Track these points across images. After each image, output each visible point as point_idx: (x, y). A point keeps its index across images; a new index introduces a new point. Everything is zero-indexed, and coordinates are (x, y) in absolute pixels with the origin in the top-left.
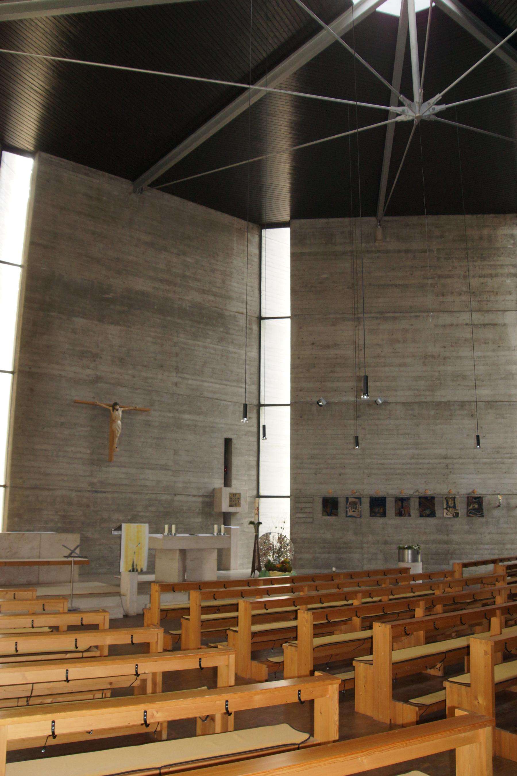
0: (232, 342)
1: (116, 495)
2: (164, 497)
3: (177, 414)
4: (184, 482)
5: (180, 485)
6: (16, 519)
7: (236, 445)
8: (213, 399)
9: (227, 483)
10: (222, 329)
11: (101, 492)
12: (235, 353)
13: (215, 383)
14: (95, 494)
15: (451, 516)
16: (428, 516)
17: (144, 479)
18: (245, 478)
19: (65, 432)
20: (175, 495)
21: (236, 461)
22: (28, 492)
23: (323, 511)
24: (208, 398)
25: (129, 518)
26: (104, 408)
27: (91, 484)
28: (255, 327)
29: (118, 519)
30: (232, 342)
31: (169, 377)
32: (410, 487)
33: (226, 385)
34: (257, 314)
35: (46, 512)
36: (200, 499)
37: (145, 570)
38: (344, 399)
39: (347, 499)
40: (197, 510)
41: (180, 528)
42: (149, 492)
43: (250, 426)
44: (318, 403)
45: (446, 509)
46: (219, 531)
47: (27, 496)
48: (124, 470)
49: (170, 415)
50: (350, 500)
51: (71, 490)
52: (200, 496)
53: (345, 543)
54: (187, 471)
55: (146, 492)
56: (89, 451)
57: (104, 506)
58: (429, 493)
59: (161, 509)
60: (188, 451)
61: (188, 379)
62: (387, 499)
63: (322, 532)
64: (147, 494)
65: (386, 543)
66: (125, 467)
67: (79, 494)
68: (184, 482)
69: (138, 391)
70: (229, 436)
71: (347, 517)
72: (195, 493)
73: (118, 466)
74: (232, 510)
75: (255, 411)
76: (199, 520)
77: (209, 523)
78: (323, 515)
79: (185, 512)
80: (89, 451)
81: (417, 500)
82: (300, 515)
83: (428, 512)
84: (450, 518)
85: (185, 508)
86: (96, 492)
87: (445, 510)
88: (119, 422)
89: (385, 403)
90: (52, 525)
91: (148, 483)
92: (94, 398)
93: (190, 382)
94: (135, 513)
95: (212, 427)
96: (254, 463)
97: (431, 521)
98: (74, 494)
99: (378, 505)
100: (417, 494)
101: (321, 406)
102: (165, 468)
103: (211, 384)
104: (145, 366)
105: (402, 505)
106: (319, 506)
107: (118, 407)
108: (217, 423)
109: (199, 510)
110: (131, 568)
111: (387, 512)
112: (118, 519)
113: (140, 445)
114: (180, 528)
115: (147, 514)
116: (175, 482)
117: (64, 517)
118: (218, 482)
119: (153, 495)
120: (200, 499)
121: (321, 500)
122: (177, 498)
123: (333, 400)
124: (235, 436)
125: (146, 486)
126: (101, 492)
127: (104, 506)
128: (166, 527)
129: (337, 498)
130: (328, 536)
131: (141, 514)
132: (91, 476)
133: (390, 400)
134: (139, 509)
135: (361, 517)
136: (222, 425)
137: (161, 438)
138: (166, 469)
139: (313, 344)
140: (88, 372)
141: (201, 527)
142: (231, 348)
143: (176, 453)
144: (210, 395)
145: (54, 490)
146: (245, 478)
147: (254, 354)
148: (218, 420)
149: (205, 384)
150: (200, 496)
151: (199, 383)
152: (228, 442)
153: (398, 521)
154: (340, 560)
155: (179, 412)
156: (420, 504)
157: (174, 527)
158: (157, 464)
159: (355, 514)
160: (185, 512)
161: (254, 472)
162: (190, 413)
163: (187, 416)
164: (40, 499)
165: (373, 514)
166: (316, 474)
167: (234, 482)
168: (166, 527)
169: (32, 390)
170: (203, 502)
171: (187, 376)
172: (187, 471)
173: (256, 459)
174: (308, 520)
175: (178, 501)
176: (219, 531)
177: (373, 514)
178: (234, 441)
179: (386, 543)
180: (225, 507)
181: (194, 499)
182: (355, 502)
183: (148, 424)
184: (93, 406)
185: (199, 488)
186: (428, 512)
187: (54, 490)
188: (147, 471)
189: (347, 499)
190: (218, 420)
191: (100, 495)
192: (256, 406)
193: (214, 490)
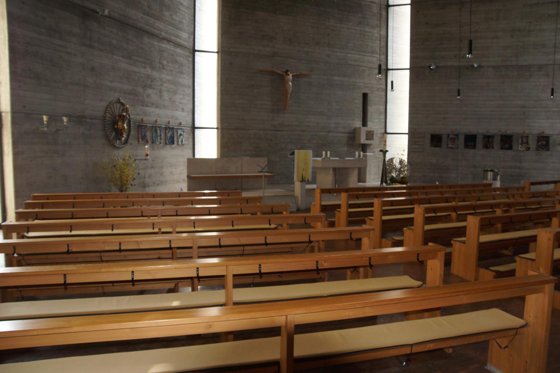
0: (368, 25)
2: (322, 134)
7: (371, 97)
8: (354, 66)
9: (364, 124)
10: (360, 15)
12: (370, 32)
13: (356, 54)
15: (524, 149)
16: (507, 149)
18: (377, 121)
20: (329, 132)
21: (371, 109)
26: (279, 74)
28: (384, 13)
30: (368, 25)
32: (496, 128)
33: (364, 55)
34: (386, 3)
36: (346, 135)
37: (310, 180)
38: (449, 64)
39: (448, 135)
43: (380, 85)
44: (430, 67)
45: (521, 144)
46: (359, 156)
50: (451, 136)
52: (346, 133)
58: (509, 133)
62: (478, 136)
65: (475, 167)
70: (366, 91)
72: (342, 130)
74: (368, 142)
76: (345, 149)
81: (499, 138)
82: (415, 146)
83: (507, 146)
84: (523, 151)
86: (277, 130)
87: (520, 146)
88: (290, 83)
89: (479, 67)
93: (338, 54)
96: (383, 111)
97: (509, 152)
99: (470, 140)
100: (500, 133)
101: (432, 69)
103: (353, 55)
105: (488, 141)
106: (428, 140)
107: (289, 73)
110: (301, 179)
111: (477, 145)
118: (358, 124)
120: (346, 135)
121: (429, 136)
122: (331, 134)
123: (440, 65)
128: (324, 153)
133: (483, 64)
135: (458, 148)
136: (361, 84)
139: (427, 23)
142: (367, 29)
144: (353, 63)
146: (377, 121)
147: (383, 33)
148: (358, 80)
149: (349, 55)
150: (346, 133)
152: (365, 96)
153: (485, 152)
156: (501, 140)
157: (329, 153)
159: (453, 146)
161: (383, 117)
163: (336, 78)
165: (466, 146)
167: (369, 123)
168: (324, 153)
169: (231, 64)
171: (336, 50)
173: (384, 107)
176: (359, 156)
177: (466, 146)
178: (369, 95)
179: (475, 167)
180: (363, 140)
181: (341, 135)
182: (454, 138)
184: (273, 73)
186: (507, 146)
187: (249, 130)
189: (448, 135)
190: (358, 80)
193: (355, 128)
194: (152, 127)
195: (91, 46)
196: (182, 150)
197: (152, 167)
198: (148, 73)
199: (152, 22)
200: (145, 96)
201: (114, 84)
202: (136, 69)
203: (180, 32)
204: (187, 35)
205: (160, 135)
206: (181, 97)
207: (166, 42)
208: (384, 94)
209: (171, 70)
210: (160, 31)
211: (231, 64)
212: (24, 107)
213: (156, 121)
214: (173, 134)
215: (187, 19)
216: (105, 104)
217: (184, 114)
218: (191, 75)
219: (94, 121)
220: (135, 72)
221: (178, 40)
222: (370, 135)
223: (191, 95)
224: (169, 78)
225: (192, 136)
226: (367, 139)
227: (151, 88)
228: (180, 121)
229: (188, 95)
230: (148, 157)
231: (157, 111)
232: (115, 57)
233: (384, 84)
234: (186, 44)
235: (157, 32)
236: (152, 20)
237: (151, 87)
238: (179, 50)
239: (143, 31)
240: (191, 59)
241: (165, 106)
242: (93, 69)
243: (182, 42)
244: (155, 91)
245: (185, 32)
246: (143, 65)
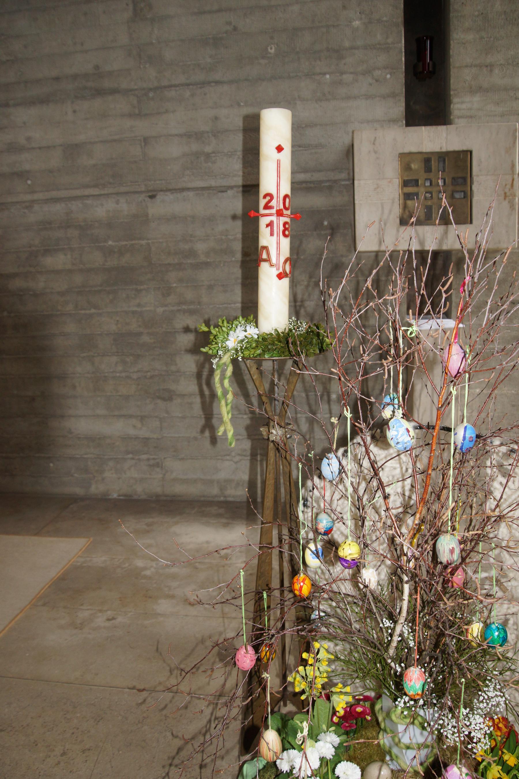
2: (102, 210)
4: (188, 136)
5: (175, 150)
42: (36, 196)
54: (203, 84)
55: (28, 197)
59: (96, 258)
68: (188, 136)
74: (431, 238)
79: (207, 264)
85: (201, 247)
91: (26, 162)
116: (146, 140)
119: (59, 208)
122: (158, 208)
125: (22, 175)
138: (99, 92)
158: (57, 79)
160: (207, 264)
172: (203, 84)
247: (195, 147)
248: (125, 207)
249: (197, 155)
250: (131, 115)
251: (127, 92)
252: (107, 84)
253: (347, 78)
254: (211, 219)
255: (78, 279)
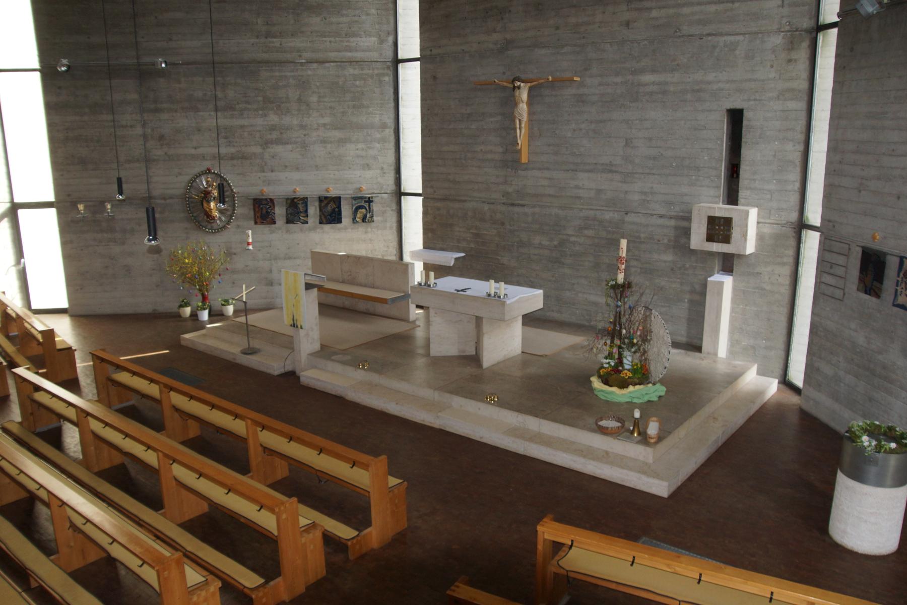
1: (537, 210)
2: (608, 216)
3: (630, 77)
5: (636, 197)
6: (430, 235)
11: (519, 205)
14: (511, 208)
17: (577, 187)
19: (473, 127)
22: (439, 204)
23: (861, 280)
24: (692, 36)
25: (556, 243)
27: (506, 194)
29: (540, 244)
31: (614, 13)
35: (457, 229)
36: (672, 223)
40: (666, 241)
41: (634, 267)
47: (439, 209)
48: (547, 174)
49: (619, 79)
51: (484, 202)
53: (884, 367)
56: (501, 150)
57: (523, 225)
60: (650, 139)
61: (650, 9)
63: (853, 326)
64: (581, 210)
66: (548, 169)
67: (492, 206)
69: (565, 50)
70: (736, 103)
71: (894, 305)
73: (540, 169)
75: (805, 44)
76: (668, 257)
77: (688, 266)
78: (858, 290)
80: (501, 150)
85: (642, 235)
86: (513, 205)
88: (523, 108)
90: (464, 244)
92: (504, 73)
94: (565, 237)
95: (698, 91)
96: (797, 157)
98: (486, 207)
102: (609, 169)
103: (697, 9)
104: (575, 6)
108: (709, 83)
109: (669, 241)
112: (540, 244)
113: (569, 135)
114: (634, 267)
115: (582, 240)
116: (626, 192)
117: (477, 235)
120: (672, 223)
124: (752, 103)
125: (579, 198)
126: (519, 205)
127: (523, 225)
129: (885, 254)
130: (861, 340)
131: (573, 239)
132: (505, 183)
134: (570, 232)
136: (721, 85)
137: (601, 122)
138: (611, 171)
140: (495, 37)
141: (672, 270)
143: (628, 143)
144: (696, 30)
145: (465, 201)
146: (772, 187)
148: (711, 77)
151: (671, 11)
152: (736, 118)
154: (871, 399)
155: (634, 72)
162: (654, 71)
163: (648, 78)
164: (451, 211)
166: (860, 191)
169: (435, 78)
170: (676, 228)
173: (801, 147)
174: (838, 293)
175: (633, 223)
178: (746, 114)
181: (661, 221)
183: (581, 100)
185: (670, 203)
187: (465, 201)
188: (581, 175)
190: (711, 77)
191: (516, 209)
192: (809, 31)
194: (287, 199)
195: (157, 110)
196: (366, 232)
197: (288, 257)
198: (273, 123)
199: (277, 45)
200: (267, 156)
201: (200, 151)
202: (245, 122)
203: (352, 39)
204: (374, 39)
205: (306, 211)
206: (360, 146)
207: (315, 65)
208: (803, 105)
209: (330, 108)
210: (299, 51)
211: (435, 78)
212: (69, 195)
213: (295, 192)
214: (339, 207)
215: (373, 11)
216: (186, 178)
217: (369, 174)
218: (392, 105)
219: (168, 201)
220: (242, 127)
221: (349, 54)
222: (720, 229)
223: (392, 138)
224: (327, 120)
225: (394, 207)
226: (710, 238)
227: (282, 144)
228: (358, 186)
229: (383, 140)
230: (251, 247)
231: (296, 175)
232: (201, 113)
233: (805, 75)
234: (374, 55)
235: (289, 56)
236: (276, 42)
237: (278, 142)
238: (351, 71)
239: (259, 62)
240: (388, 79)
241: (317, 166)
242: (161, 138)
243: (358, 55)
244: (289, 147)
245: (370, 36)
246: (260, 112)
247: (643, 197)
248: (616, 216)
249: (644, 200)
250: (622, 182)
251: (621, 173)
252: (613, 168)
253: (701, 178)
254: (647, 225)
255: (596, 241)
